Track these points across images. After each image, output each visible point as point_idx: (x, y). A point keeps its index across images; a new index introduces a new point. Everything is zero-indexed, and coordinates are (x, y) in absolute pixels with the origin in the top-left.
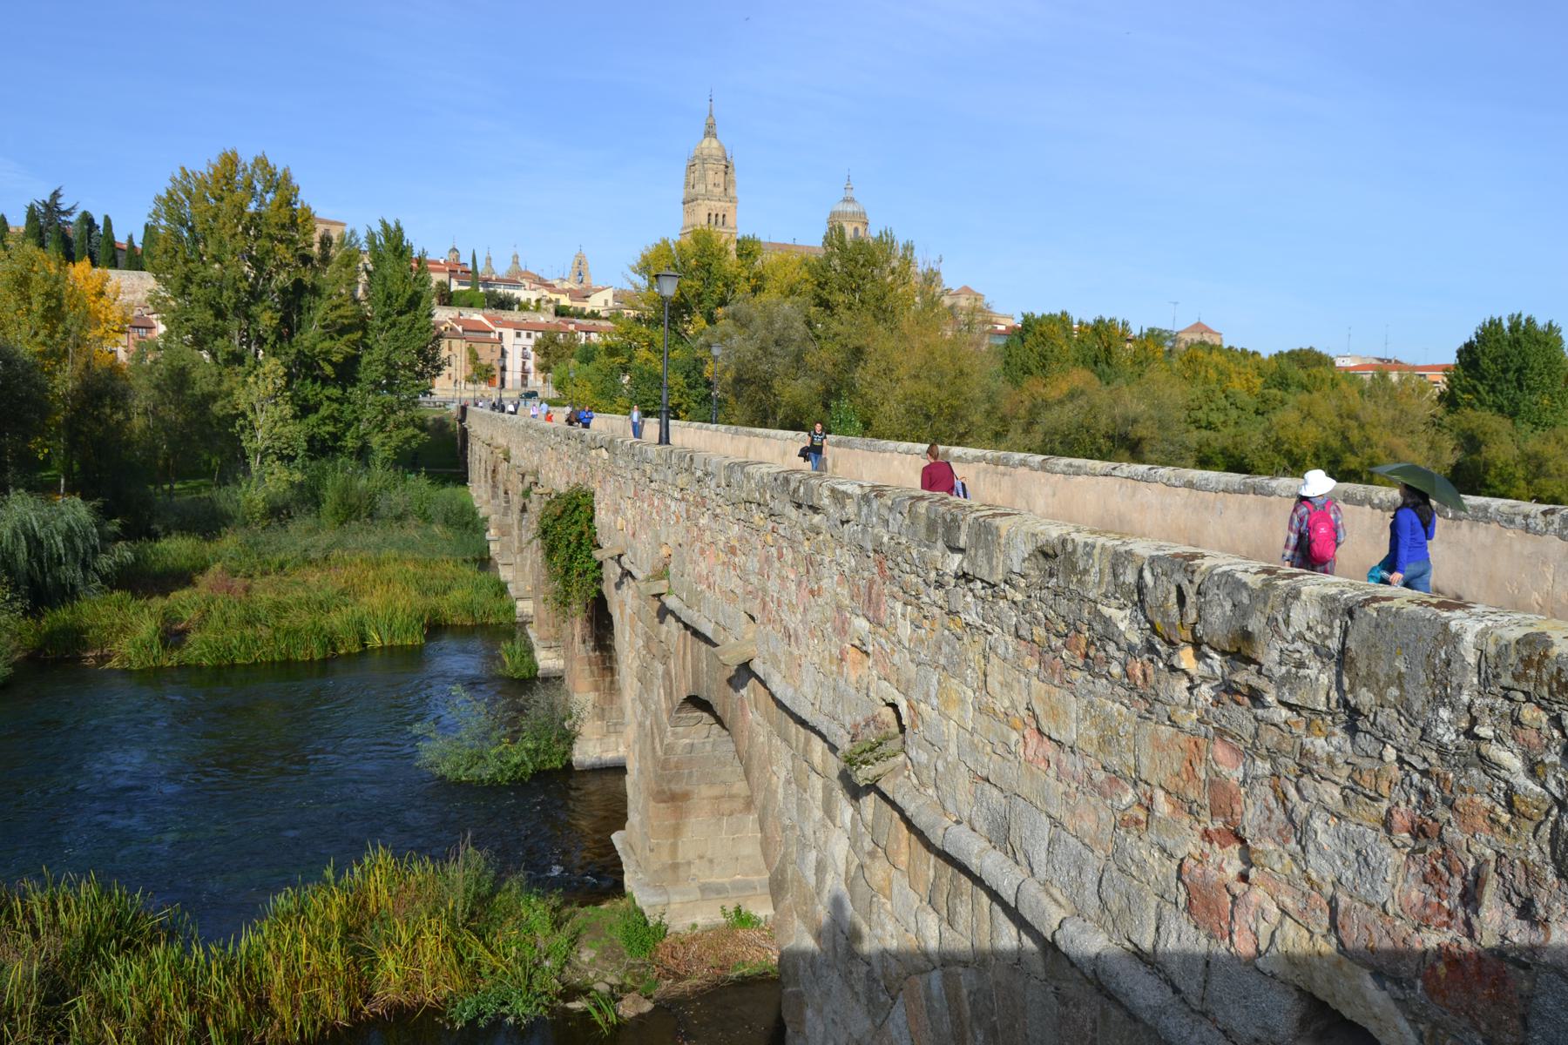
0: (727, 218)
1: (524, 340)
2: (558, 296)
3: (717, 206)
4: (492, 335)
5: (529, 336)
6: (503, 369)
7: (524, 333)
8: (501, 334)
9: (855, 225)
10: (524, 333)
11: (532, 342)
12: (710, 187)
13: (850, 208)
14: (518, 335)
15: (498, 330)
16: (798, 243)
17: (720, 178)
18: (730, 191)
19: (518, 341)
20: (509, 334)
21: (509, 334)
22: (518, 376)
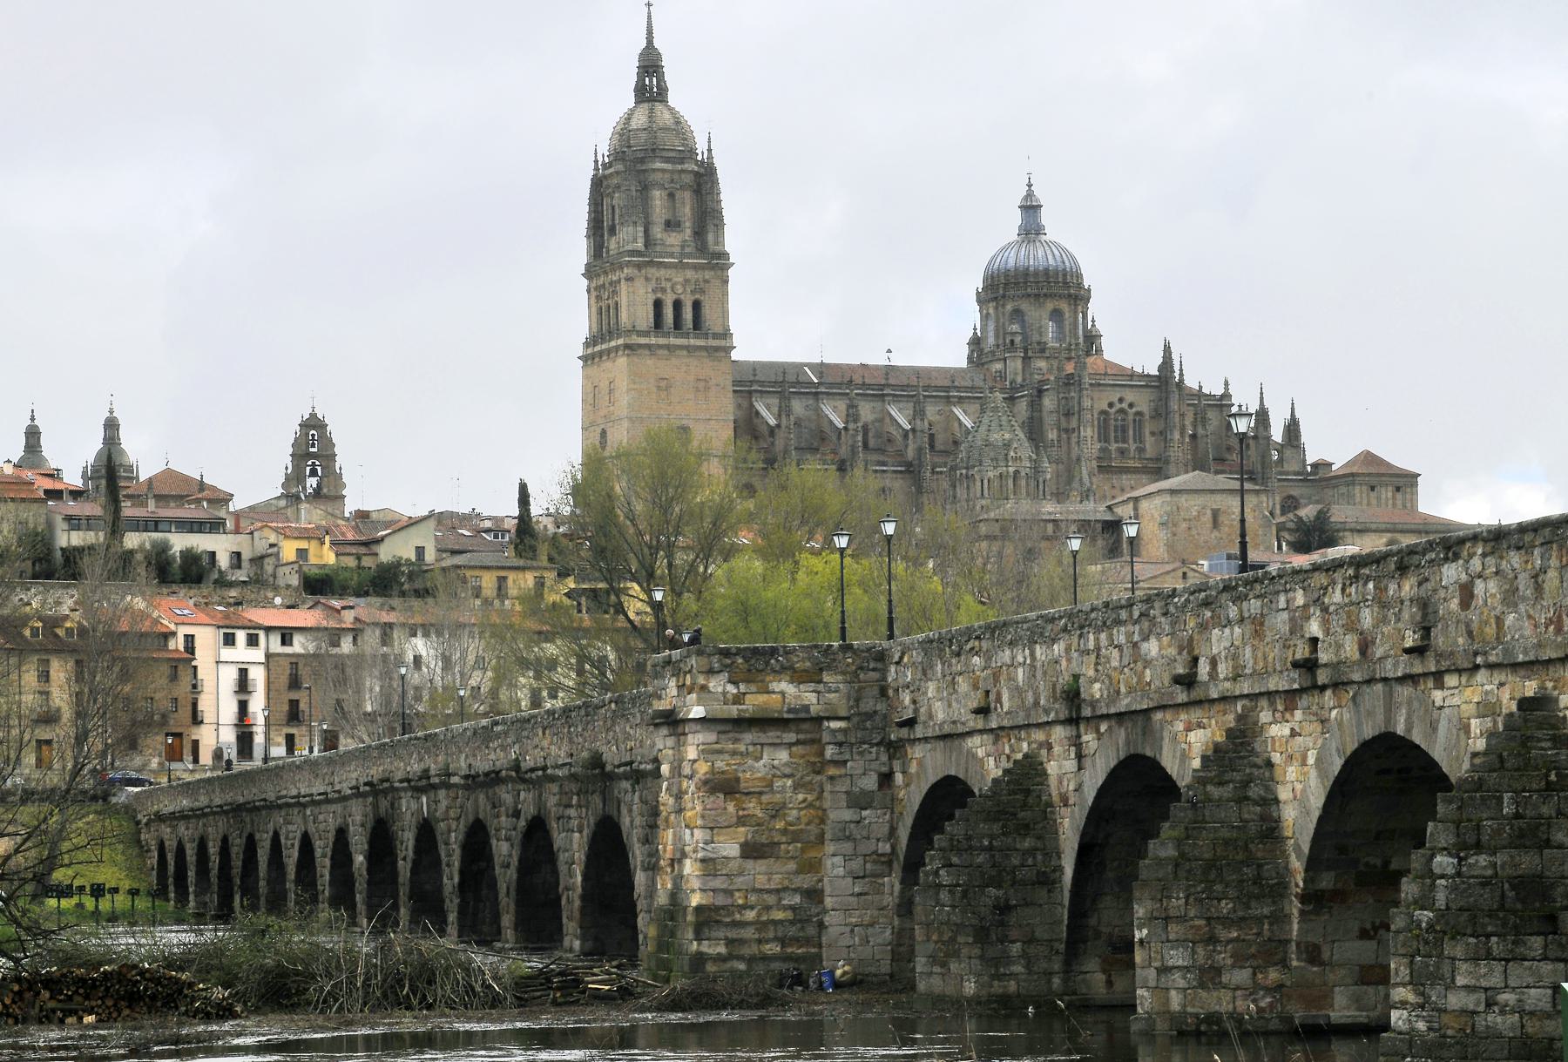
0: (708, 312)
1: (241, 652)
2: (303, 545)
3: (678, 285)
4: (172, 645)
5: (252, 641)
6: (196, 720)
7: (241, 636)
8: (189, 639)
9: (1050, 305)
10: (241, 636)
11: (258, 655)
12: (658, 232)
13: (1038, 257)
14: (229, 640)
15: (189, 630)
16: (899, 360)
17: (686, 211)
18: (710, 237)
19: (227, 654)
20: (206, 639)
21: (206, 639)
22: (229, 736)
